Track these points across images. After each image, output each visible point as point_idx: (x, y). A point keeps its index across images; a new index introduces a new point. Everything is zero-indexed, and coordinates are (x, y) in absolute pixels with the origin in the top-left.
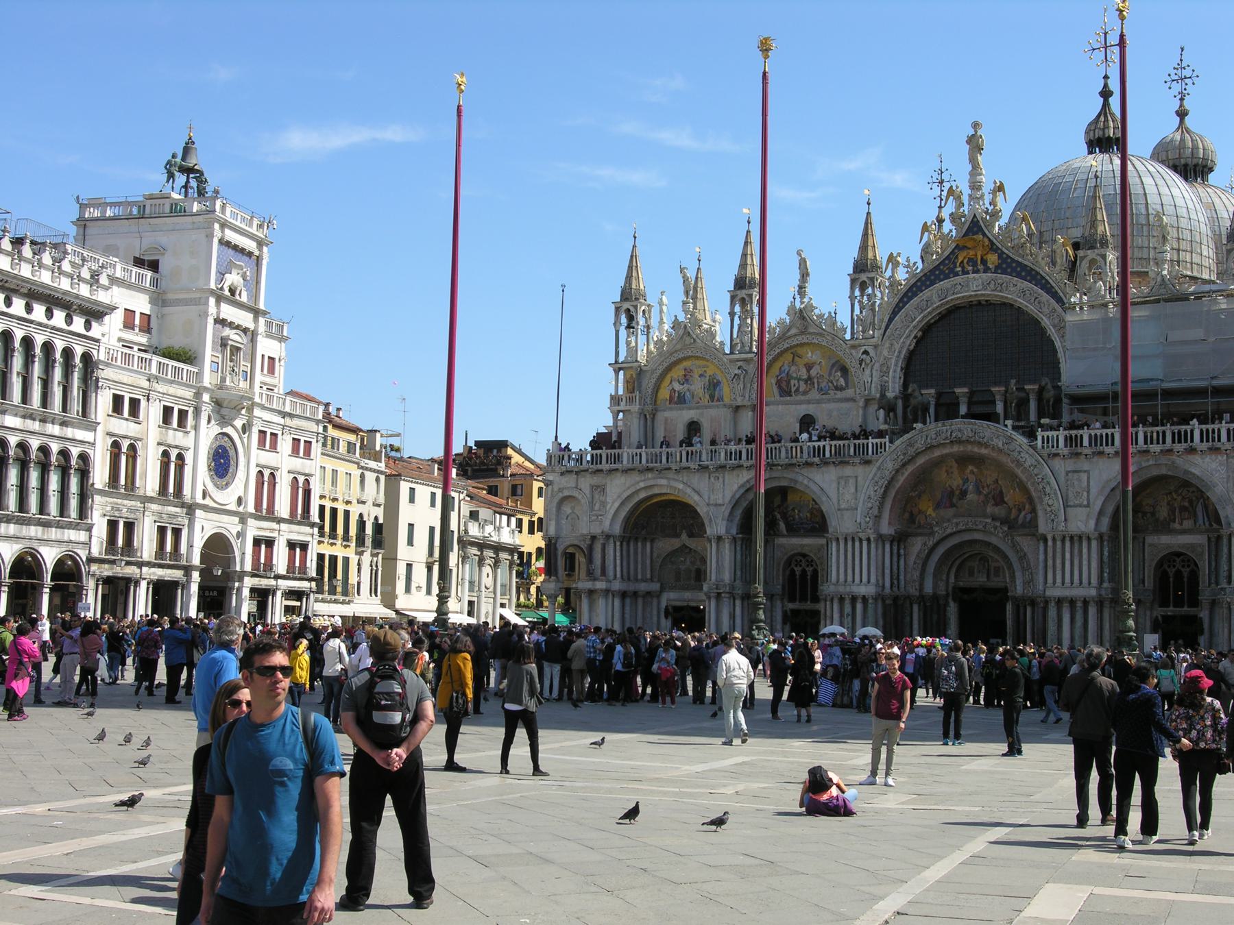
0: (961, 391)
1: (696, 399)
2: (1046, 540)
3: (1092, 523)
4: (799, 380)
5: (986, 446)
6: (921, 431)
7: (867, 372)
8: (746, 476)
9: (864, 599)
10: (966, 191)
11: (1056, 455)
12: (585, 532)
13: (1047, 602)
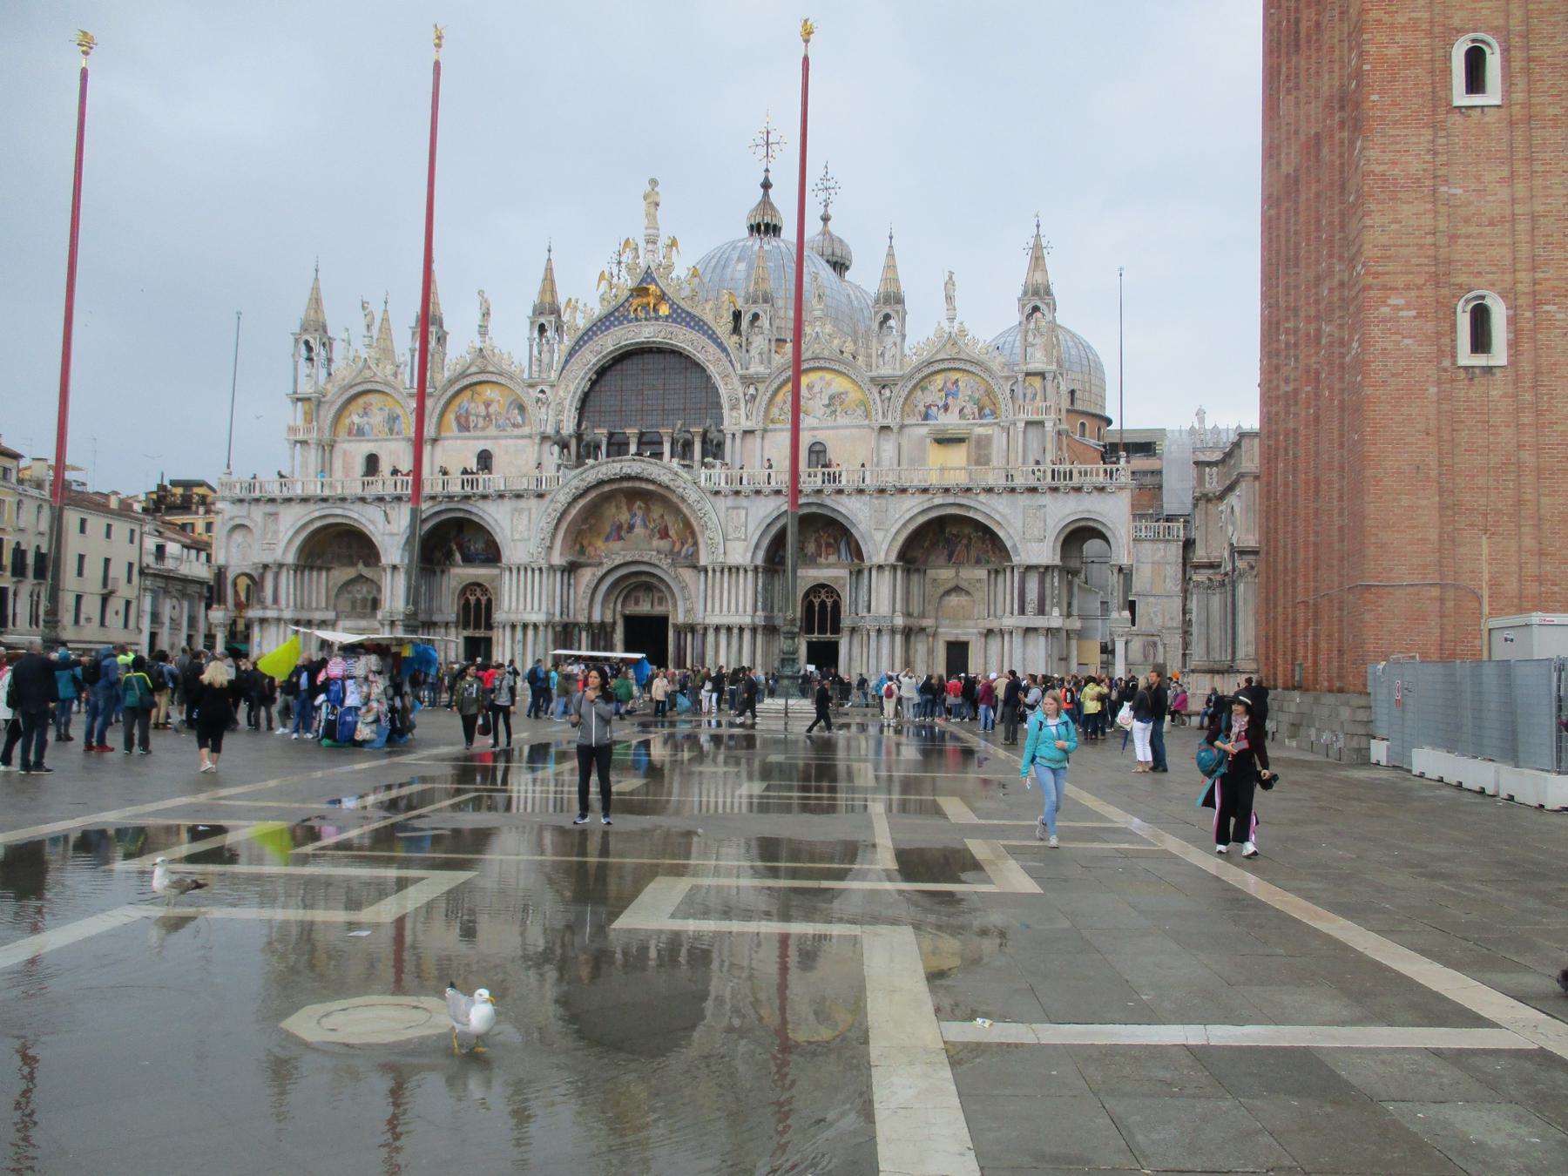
0: (632, 431)
2: (706, 571)
3: (749, 555)
5: (653, 482)
6: (593, 467)
7: (544, 409)
9: (535, 626)
10: (642, 245)
11: (717, 493)
13: (705, 629)
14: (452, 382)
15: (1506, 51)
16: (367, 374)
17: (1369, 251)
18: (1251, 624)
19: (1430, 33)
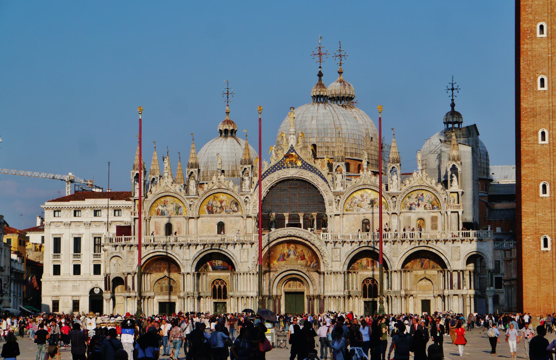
0: (286, 214)
1: (170, 213)
2: (324, 274)
3: (342, 267)
4: (217, 207)
7: (248, 205)
8: (200, 248)
12: (124, 271)
14: (205, 193)
15: (550, 185)
16: (167, 189)
17: (523, 227)
18: (515, 299)
19: (534, 182)
